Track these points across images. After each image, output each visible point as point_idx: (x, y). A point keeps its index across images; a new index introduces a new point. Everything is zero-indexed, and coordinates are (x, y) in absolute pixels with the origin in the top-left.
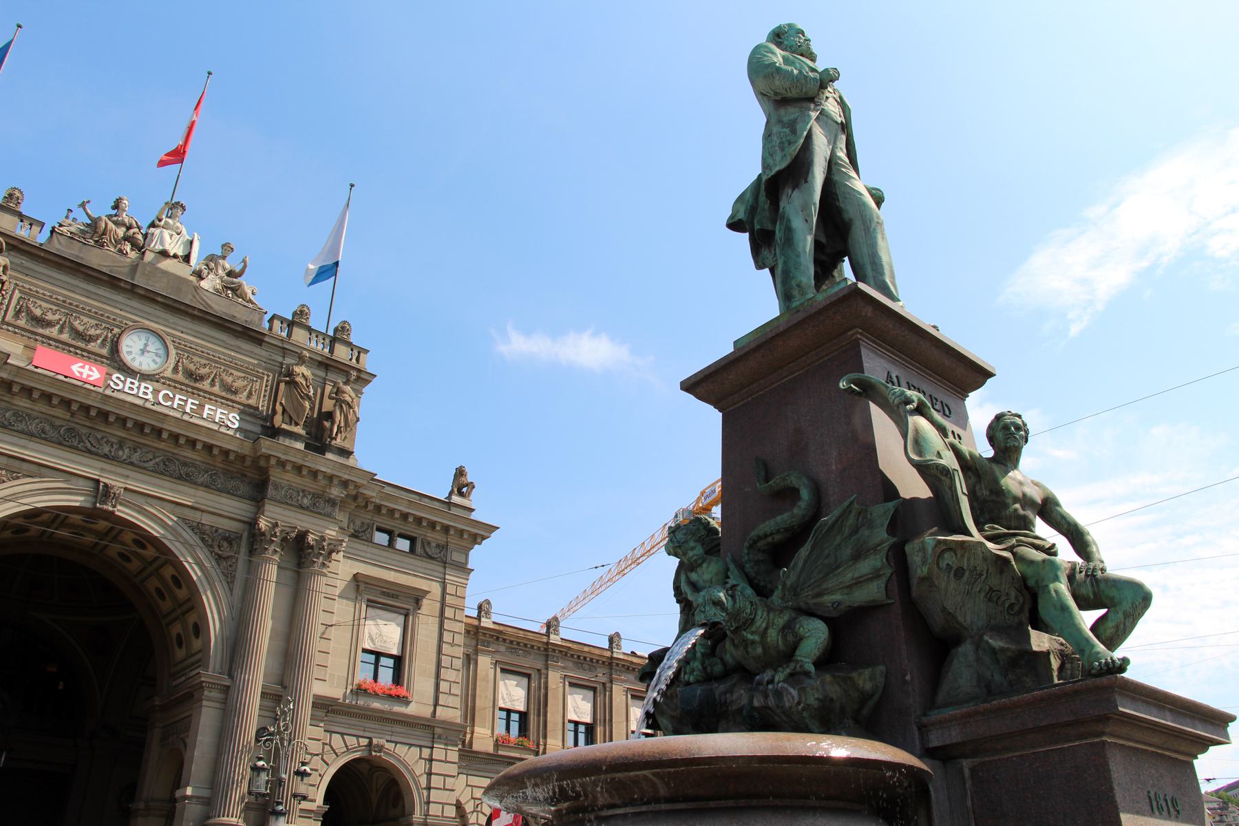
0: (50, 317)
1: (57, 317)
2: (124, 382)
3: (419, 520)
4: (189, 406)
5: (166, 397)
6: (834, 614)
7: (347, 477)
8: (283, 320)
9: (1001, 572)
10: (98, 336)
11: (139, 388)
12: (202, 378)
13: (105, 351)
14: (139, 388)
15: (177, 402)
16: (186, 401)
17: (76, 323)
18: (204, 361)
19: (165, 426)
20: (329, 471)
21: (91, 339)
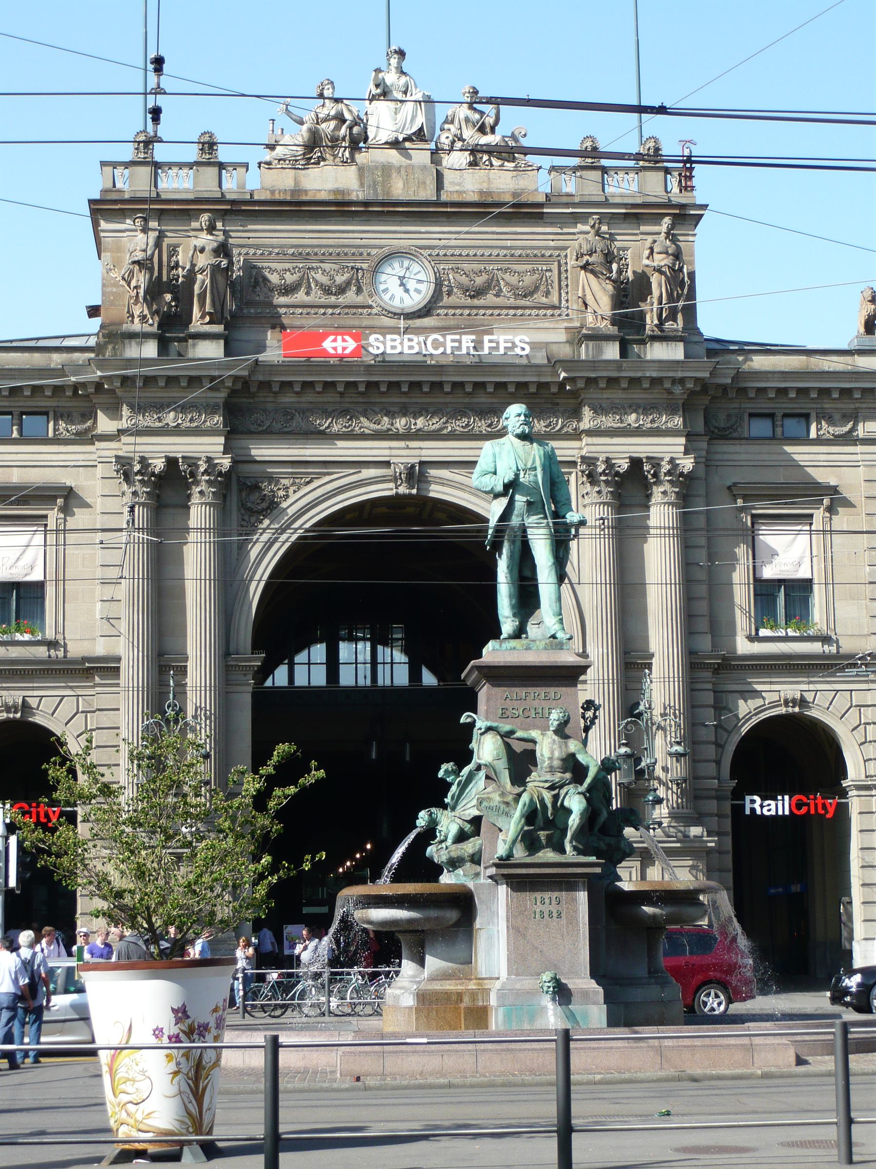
0: (290, 279)
1: (295, 277)
2: (384, 343)
3: (803, 392)
4: (464, 346)
5: (436, 344)
7: (680, 374)
10: (348, 283)
11: (402, 343)
12: (479, 292)
13: (359, 300)
14: (402, 343)
15: (449, 345)
16: (460, 341)
17: (319, 276)
18: (477, 267)
19: (444, 379)
20: (654, 374)
21: (342, 290)
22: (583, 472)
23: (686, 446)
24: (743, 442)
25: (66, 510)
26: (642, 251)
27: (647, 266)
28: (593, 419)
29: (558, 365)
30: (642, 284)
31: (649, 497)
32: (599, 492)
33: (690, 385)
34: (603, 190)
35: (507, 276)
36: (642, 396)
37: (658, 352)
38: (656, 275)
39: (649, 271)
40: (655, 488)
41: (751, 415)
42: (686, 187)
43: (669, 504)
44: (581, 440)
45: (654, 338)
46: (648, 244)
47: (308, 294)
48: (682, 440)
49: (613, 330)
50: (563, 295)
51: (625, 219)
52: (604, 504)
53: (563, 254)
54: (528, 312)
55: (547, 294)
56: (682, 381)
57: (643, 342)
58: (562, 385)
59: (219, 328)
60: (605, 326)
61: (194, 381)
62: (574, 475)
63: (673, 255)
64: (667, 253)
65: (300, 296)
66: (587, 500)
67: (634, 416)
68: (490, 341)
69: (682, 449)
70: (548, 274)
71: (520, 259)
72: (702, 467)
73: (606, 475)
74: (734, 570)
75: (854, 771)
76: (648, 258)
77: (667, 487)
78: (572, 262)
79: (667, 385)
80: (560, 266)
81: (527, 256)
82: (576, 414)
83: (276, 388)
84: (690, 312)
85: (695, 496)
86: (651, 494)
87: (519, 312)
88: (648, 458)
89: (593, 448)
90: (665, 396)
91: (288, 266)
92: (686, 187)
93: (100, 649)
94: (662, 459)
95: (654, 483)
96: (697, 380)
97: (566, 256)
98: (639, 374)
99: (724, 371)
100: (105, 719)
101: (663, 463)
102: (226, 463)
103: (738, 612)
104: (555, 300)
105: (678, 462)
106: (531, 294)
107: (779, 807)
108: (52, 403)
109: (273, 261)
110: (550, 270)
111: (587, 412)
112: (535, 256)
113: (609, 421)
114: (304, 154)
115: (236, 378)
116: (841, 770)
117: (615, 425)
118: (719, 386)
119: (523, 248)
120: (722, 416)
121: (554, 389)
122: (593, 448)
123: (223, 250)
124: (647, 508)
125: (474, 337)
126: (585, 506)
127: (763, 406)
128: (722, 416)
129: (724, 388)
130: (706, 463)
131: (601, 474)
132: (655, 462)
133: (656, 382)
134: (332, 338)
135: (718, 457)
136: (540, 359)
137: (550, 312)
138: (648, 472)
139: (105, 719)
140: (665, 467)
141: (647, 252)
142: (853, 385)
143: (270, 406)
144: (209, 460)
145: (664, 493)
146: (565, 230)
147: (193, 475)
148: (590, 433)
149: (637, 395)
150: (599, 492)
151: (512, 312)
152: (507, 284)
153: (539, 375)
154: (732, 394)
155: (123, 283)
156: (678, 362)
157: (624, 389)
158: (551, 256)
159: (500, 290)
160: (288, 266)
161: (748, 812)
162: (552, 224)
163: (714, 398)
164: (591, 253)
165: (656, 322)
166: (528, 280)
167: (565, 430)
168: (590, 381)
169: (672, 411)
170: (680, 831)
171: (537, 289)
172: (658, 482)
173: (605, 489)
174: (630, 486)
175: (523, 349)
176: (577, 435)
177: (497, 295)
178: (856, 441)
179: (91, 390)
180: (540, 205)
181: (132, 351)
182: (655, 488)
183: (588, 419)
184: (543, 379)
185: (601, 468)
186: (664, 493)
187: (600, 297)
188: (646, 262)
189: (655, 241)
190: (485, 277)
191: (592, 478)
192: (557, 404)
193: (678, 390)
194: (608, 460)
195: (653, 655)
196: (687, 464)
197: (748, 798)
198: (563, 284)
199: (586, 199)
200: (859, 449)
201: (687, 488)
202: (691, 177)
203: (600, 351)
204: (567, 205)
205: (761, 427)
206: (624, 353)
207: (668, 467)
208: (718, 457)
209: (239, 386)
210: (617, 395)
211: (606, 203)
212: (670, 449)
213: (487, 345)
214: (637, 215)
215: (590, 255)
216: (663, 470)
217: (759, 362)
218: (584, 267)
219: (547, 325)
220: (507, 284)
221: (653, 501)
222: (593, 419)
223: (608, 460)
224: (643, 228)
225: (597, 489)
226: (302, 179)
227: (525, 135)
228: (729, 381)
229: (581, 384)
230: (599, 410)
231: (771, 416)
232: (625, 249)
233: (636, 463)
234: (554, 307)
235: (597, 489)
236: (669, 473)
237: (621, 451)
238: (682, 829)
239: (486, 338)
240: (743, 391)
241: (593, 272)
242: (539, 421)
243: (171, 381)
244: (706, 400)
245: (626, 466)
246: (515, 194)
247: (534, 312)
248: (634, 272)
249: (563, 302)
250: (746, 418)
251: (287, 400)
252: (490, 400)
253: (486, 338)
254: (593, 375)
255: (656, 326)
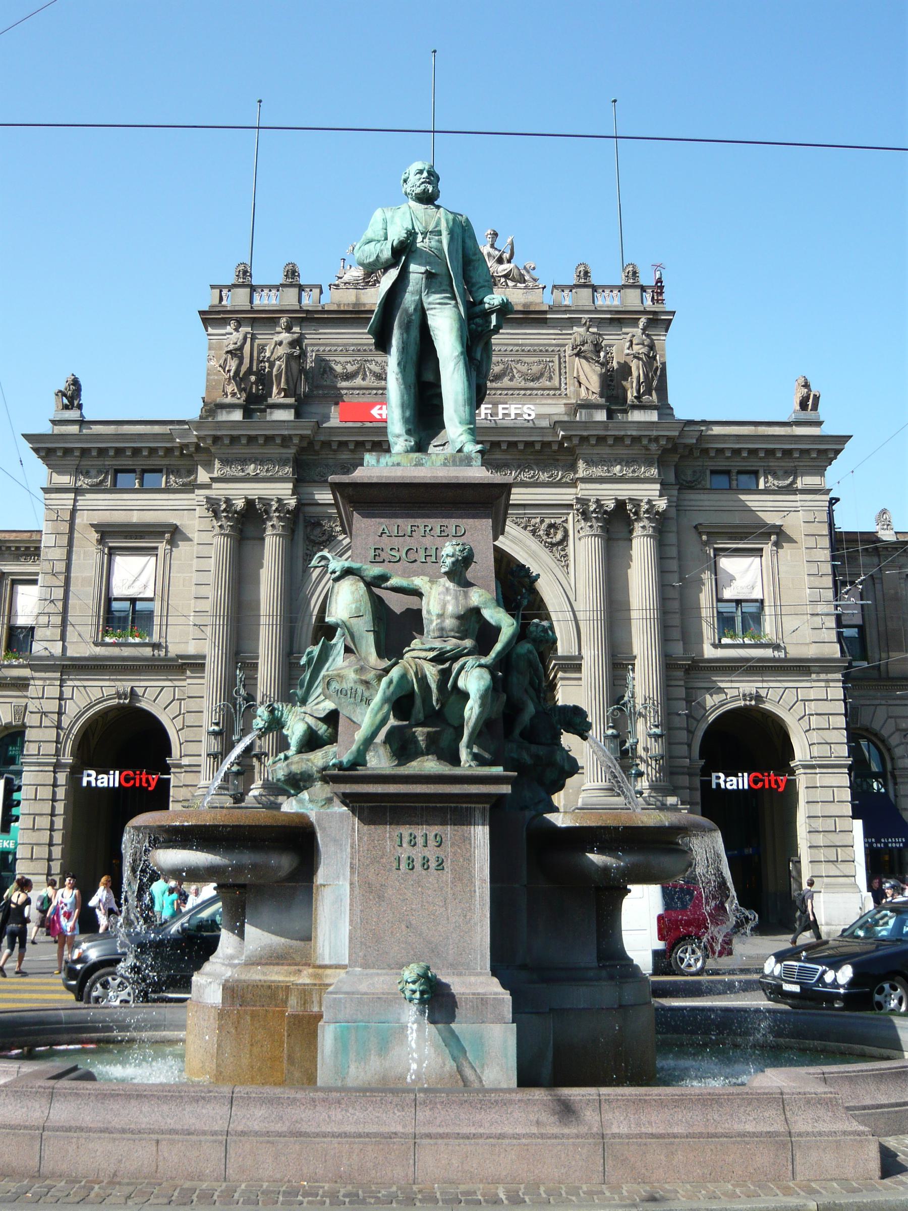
0: (350, 368)
1: (355, 367)
3: (753, 452)
6: (322, 716)
7: (655, 433)
8: (562, 288)
9: (368, 688)
17: (373, 367)
20: (634, 433)
22: (578, 510)
23: (660, 491)
24: (706, 491)
25: (172, 543)
26: (622, 346)
27: (628, 355)
28: (586, 469)
29: (557, 425)
30: (625, 370)
31: (631, 532)
32: (591, 527)
33: (663, 442)
34: (594, 302)
35: (519, 366)
36: (626, 452)
37: (637, 416)
38: (635, 360)
39: (629, 359)
40: (636, 524)
41: (713, 472)
42: (658, 300)
43: (648, 536)
44: (576, 487)
45: (634, 407)
46: (628, 337)
47: (364, 379)
48: (658, 486)
49: (602, 401)
50: (563, 379)
51: (610, 323)
52: (595, 536)
53: (562, 349)
54: (535, 392)
55: (550, 378)
56: (657, 439)
57: (625, 412)
58: (561, 444)
59: (291, 400)
60: (595, 398)
61: (269, 439)
62: (571, 515)
63: (648, 346)
64: (643, 344)
65: (358, 381)
66: (582, 534)
67: (618, 467)
68: (503, 409)
69: (657, 493)
70: (551, 364)
71: (529, 353)
72: (673, 510)
73: (597, 513)
74: (701, 592)
75: (801, 752)
76: (628, 349)
77: (645, 522)
78: (569, 351)
79: (645, 442)
80: (560, 358)
81: (535, 351)
82: (573, 468)
83: (335, 447)
84: (662, 390)
85: (670, 532)
86: (633, 529)
87: (529, 392)
88: (630, 499)
89: (586, 493)
90: (644, 452)
91: (348, 359)
92: (658, 300)
93: (191, 649)
94: (641, 501)
95: (636, 520)
96: (668, 438)
97: (565, 351)
98: (622, 433)
99: (691, 433)
100: (193, 705)
101: (642, 504)
102: (292, 502)
103: (704, 625)
104: (557, 384)
105: (654, 503)
106: (538, 379)
107: (740, 782)
108: (165, 462)
109: (338, 355)
110: (552, 361)
111: (581, 465)
112: (541, 351)
113: (598, 471)
114: (364, 279)
115: (302, 437)
116: (789, 752)
117: (604, 475)
118: (686, 446)
119: (531, 345)
120: (689, 472)
121: (555, 447)
122: (586, 493)
123: (296, 343)
124: (631, 540)
125: (490, 406)
126: (580, 539)
127: (721, 464)
128: (689, 472)
129: (690, 448)
130: (677, 506)
131: (592, 512)
132: (636, 503)
133: (636, 439)
134: (379, 407)
135: (686, 503)
136: (545, 423)
137: (552, 392)
138: (631, 510)
139: (193, 705)
140: (644, 507)
141: (628, 344)
142: (793, 446)
143: (331, 462)
144: (279, 500)
145: (644, 527)
146: (564, 332)
147: (267, 512)
148: (584, 480)
149: (621, 451)
150: (591, 527)
151: (522, 392)
152: (519, 371)
153: (543, 436)
154: (697, 453)
155: (220, 369)
156: (653, 423)
157: (610, 446)
158: (553, 351)
159: (514, 376)
160: (348, 359)
161: (714, 786)
162: (554, 327)
163: (681, 457)
164: (583, 343)
165: (635, 394)
166: (535, 369)
167: (564, 480)
168: (584, 439)
169: (650, 464)
170: (658, 800)
171: (542, 375)
172: (639, 519)
173: (596, 525)
174: (615, 523)
175: (529, 415)
176: (573, 484)
177: (511, 380)
178: (796, 492)
179: (192, 449)
180: (545, 312)
181: (223, 416)
182: (636, 524)
183: (582, 470)
184: (546, 439)
185: (593, 507)
186: (644, 527)
187: (590, 377)
188: (627, 351)
189: (633, 336)
190: (501, 366)
191: (585, 515)
192: (558, 460)
193: (653, 447)
194: (598, 501)
195: (635, 657)
196: (662, 504)
197: (714, 775)
198: (563, 371)
199: (580, 308)
200: (799, 497)
201: (662, 525)
202: (661, 293)
203: (592, 416)
204: (565, 312)
205: (722, 480)
206: (610, 416)
207: (646, 507)
208: (686, 503)
209: (305, 444)
210: (604, 451)
211: (596, 311)
212: (648, 493)
213: (501, 412)
214: (620, 319)
215: (583, 345)
216: (643, 510)
217: (717, 430)
218: (578, 355)
219: (550, 401)
220: (519, 371)
221: (635, 534)
222: (586, 469)
223: (598, 501)
224: (625, 330)
225: (589, 524)
226: (362, 296)
227: (534, 268)
228: (694, 441)
229: (576, 441)
230: (590, 463)
231: (727, 473)
232: (611, 346)
233: (621, 504)
234: (555, 389)
235: (589, 524)
236: (647, 512)
237: (609, 494)
238: (660, 798)
239: (500, 407)
240: (705, 451)
241: (585, 358)
242: (543, 473)
243: (252, 439)
244: (676, 458)
245: (612, 506)
246: (524, 305)
247: (539, 392)
248: (618, 363)
249: (563, 385)
250: (708, 472)
251: (344, 457)
252: (503, 457)
253: (500, 407)
254: (585, 433)
255: (635, 397)
